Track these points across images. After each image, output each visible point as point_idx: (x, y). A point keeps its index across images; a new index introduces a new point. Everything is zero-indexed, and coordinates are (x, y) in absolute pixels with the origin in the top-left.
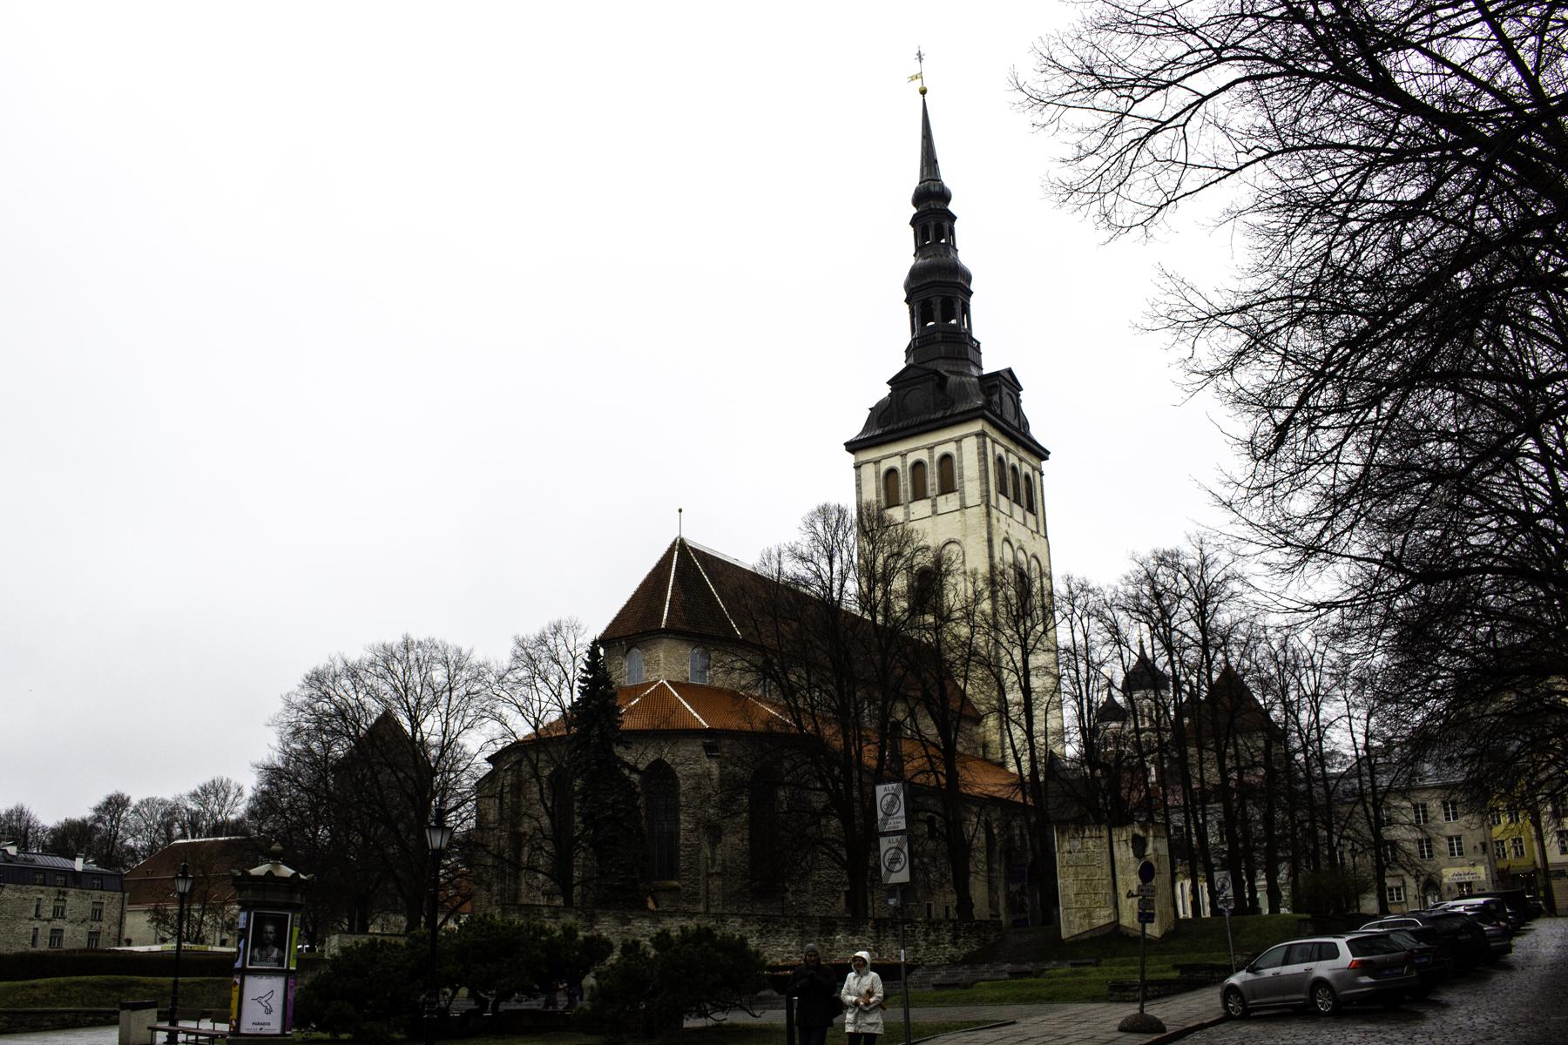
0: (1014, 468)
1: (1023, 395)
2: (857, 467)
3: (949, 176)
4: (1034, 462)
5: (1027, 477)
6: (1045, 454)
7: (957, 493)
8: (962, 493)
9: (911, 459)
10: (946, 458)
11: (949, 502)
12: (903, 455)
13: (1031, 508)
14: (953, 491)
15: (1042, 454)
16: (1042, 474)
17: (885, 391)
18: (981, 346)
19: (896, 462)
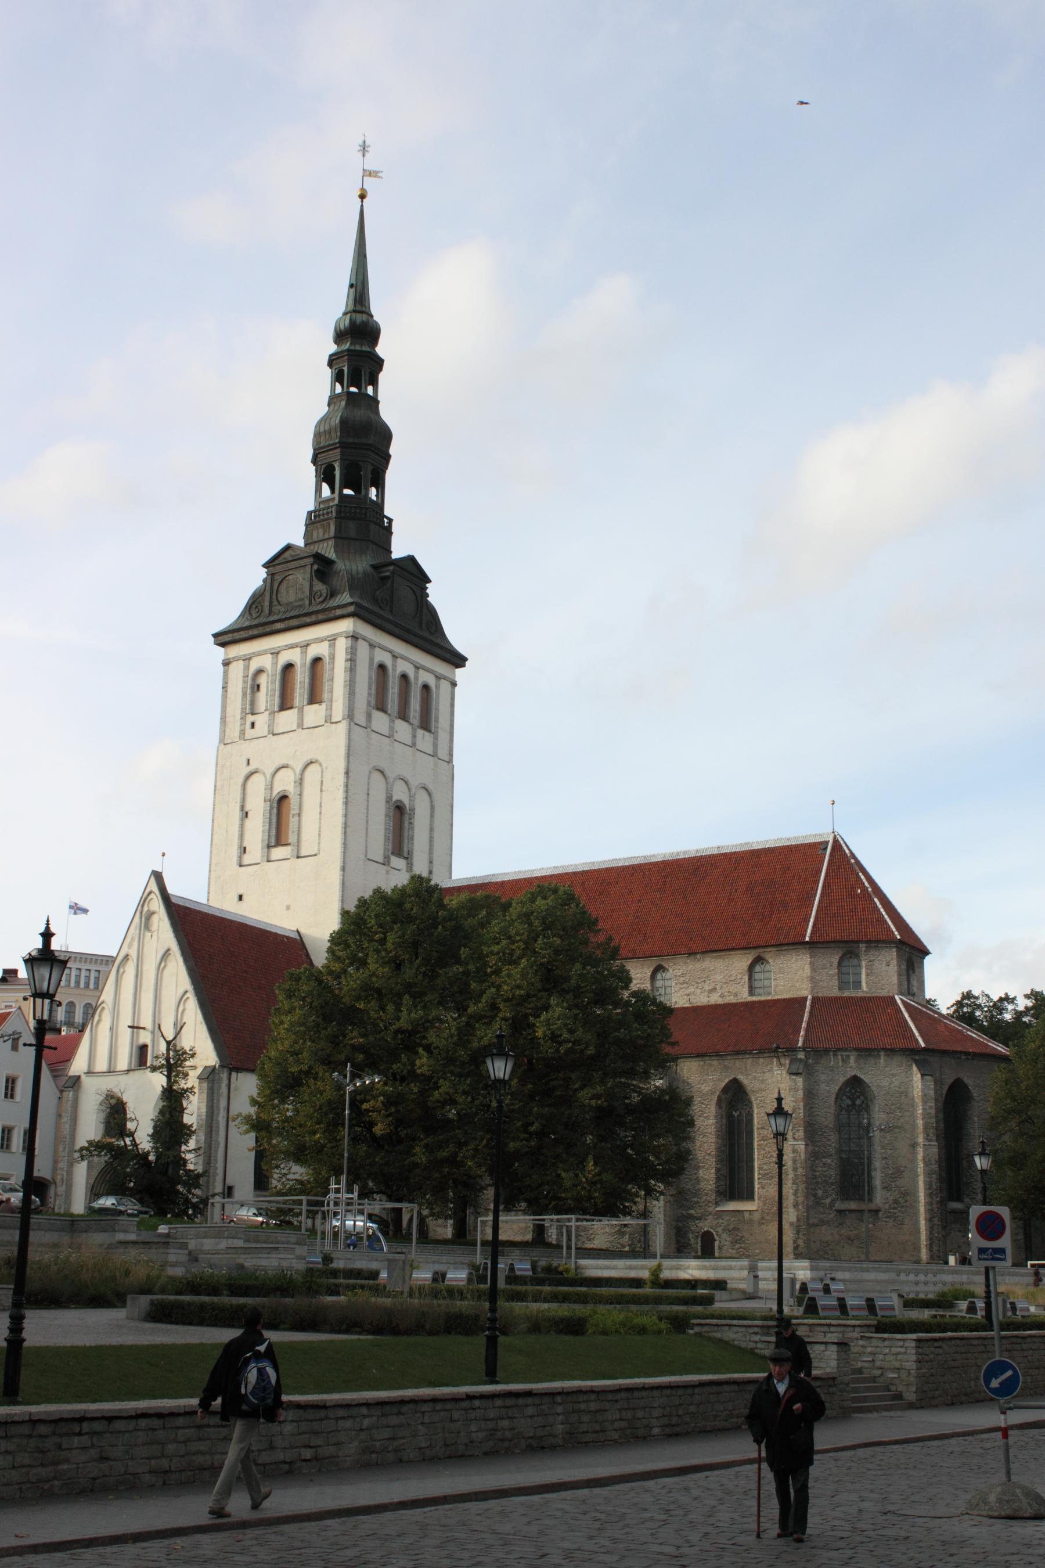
0: (404, 677)
1: (431, 589)
2: (226, 663)
3: (379, 310)
4: (440, 667)
5: (426, 687)
6: (457, 661)
7: (324, 705)
8: (330, 708)
9: (284, 658)
10: (317, 660)
11: (314, 713)
12: (276, 653)
13: (426, 724)
14: (320, 702)
15: (458, 660)
16: (454, 684)
17: (263, 573)
18: (394, 524)
19: (266, 662)
